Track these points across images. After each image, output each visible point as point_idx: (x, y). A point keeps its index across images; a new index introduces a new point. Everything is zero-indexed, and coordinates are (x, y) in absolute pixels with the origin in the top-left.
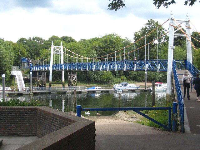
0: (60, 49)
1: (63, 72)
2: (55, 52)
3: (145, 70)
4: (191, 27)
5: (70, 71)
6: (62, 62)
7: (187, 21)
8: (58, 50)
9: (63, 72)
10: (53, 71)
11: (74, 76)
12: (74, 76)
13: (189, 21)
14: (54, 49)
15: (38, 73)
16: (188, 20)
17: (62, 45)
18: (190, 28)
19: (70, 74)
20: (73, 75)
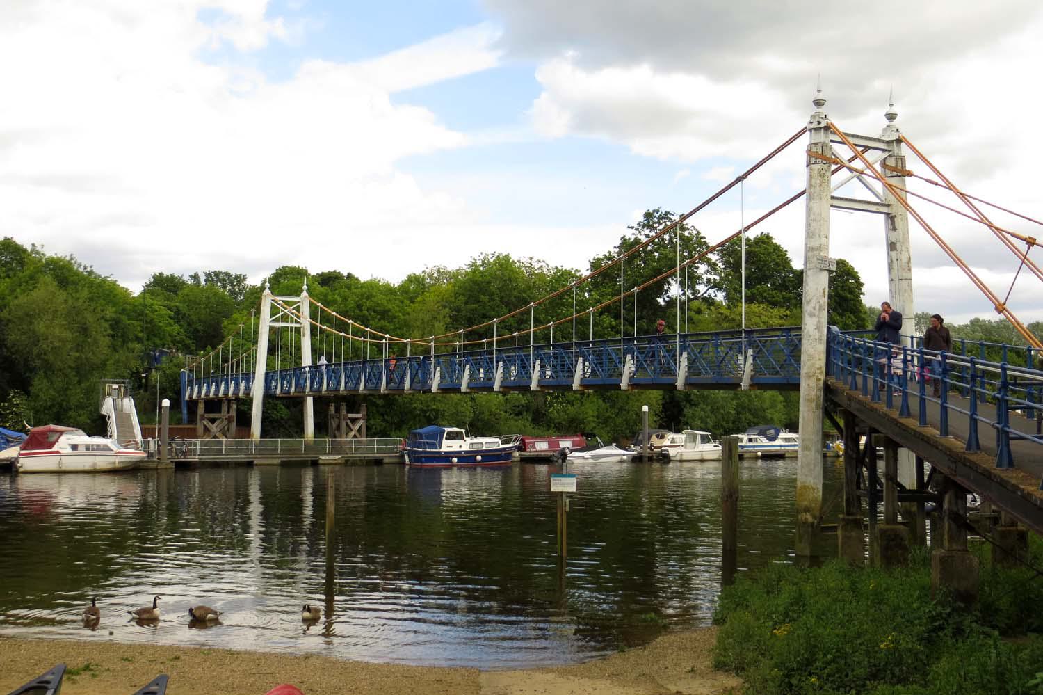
0: (298, 309)
1: (310, 400)
2: (274, 321)
4: (908, 167)
5: (339, 399)
6: (307, 360)
7: (888, 142)
10: (268, 397)
11: (354, 421)
12: (354, 421)
13: (899, 141)
14: (274, 310)
15: (201, 406)
16: (894, 137)
17: (305, 294)
18: (910, 174)
19: (338, 410)
20: (350, 416)
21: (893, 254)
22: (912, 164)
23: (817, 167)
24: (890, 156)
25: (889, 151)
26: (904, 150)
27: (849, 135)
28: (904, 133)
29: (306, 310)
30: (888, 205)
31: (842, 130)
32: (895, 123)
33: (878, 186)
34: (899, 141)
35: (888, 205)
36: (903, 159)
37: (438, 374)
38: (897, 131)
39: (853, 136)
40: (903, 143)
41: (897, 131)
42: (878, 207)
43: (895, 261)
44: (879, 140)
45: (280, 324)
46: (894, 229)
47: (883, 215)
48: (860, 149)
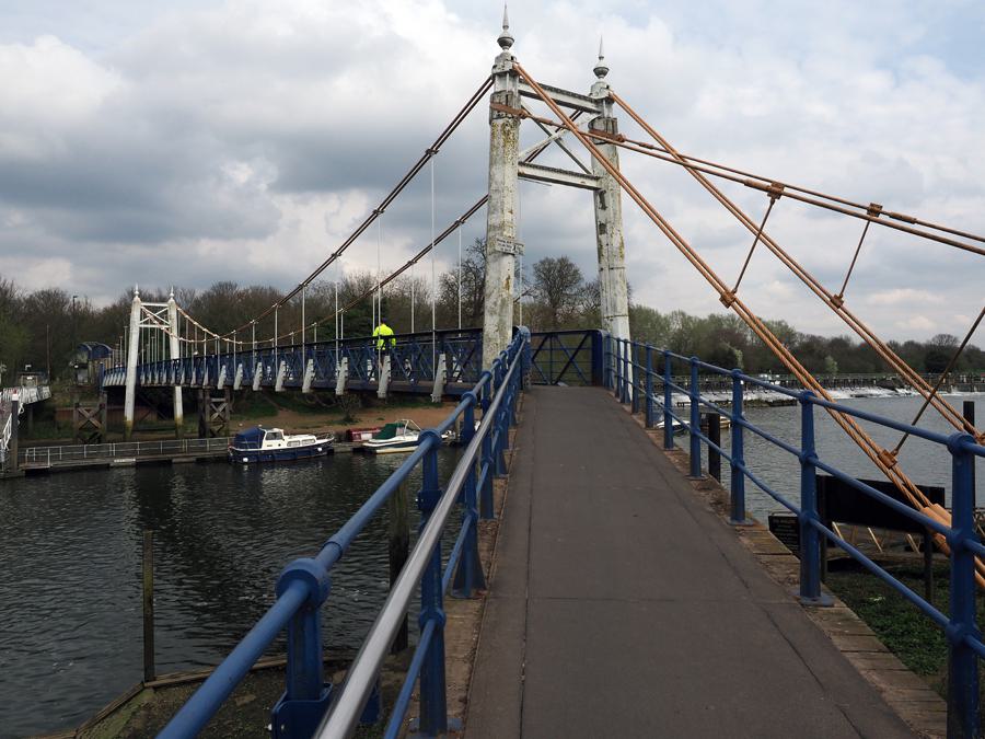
1: (178, 390)
3: (432, 388)
4: (621, 130)
7: (597, 102)
8: (150, 315)
9: (178, 390)
10: (138, 386)
13: (610, 100)
14: (143, 316)
16: (604, 94)
17: (172, 300)
18: (621, 140)
20: (214, 400)
21: (603, 237)
22: (627, 127)
23: (500, 122)
24: (599, 118)
25: (599, 113)
26: (615, 111)
27: (544, 87)
28: (616, 91)
29: (173, 314)
30: (597, 179)
31: (536, 79)
32: (606, 80)
33: (585, 156)
34: (610, 100)
35: (597, 179)
36: (614, 121)
37: (310, 368)
38: (608, 87)
39: (551, 89)
40: (615, 103)
41: (608, 87)
42: (584, 180)
43: (605, 247)
44: (584, 98)
45: (143, 326)
46: (604, 208)
47: (592, 192)
48: (569, 112)
